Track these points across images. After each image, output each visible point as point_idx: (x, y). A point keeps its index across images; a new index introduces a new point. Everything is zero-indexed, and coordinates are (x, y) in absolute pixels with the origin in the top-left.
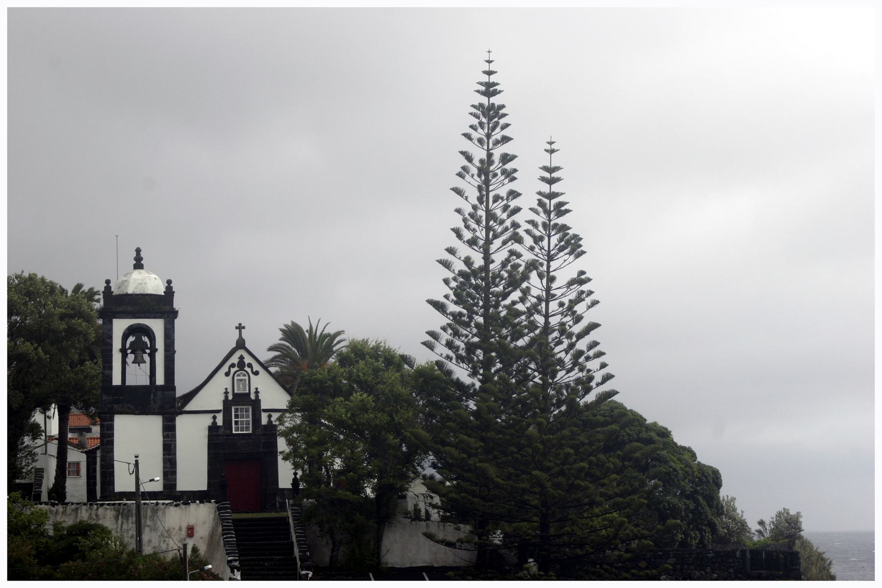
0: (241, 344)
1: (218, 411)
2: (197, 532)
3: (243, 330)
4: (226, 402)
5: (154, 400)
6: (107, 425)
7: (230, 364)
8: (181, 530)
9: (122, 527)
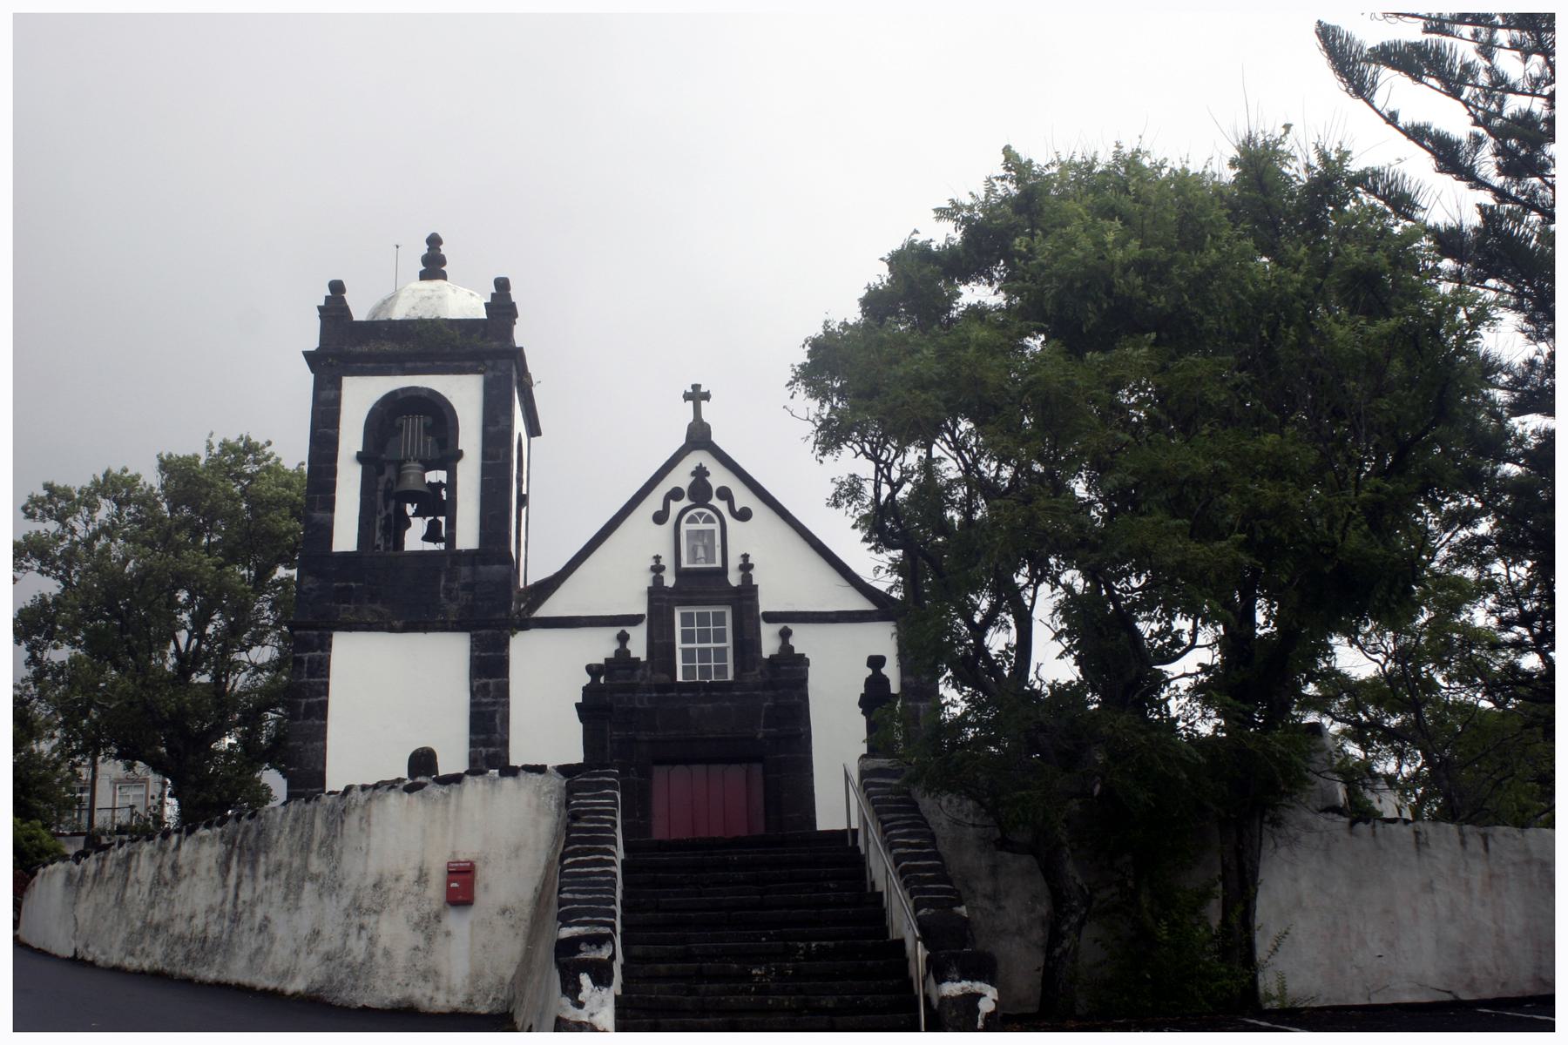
0: (699, 437)
1: (634, 620)
2: (486, 887)
3: (704, 403)
4: (656, 593)
5: (449, 591)
7: (669, 489)
8: (427, 881)
9: (237, 896)
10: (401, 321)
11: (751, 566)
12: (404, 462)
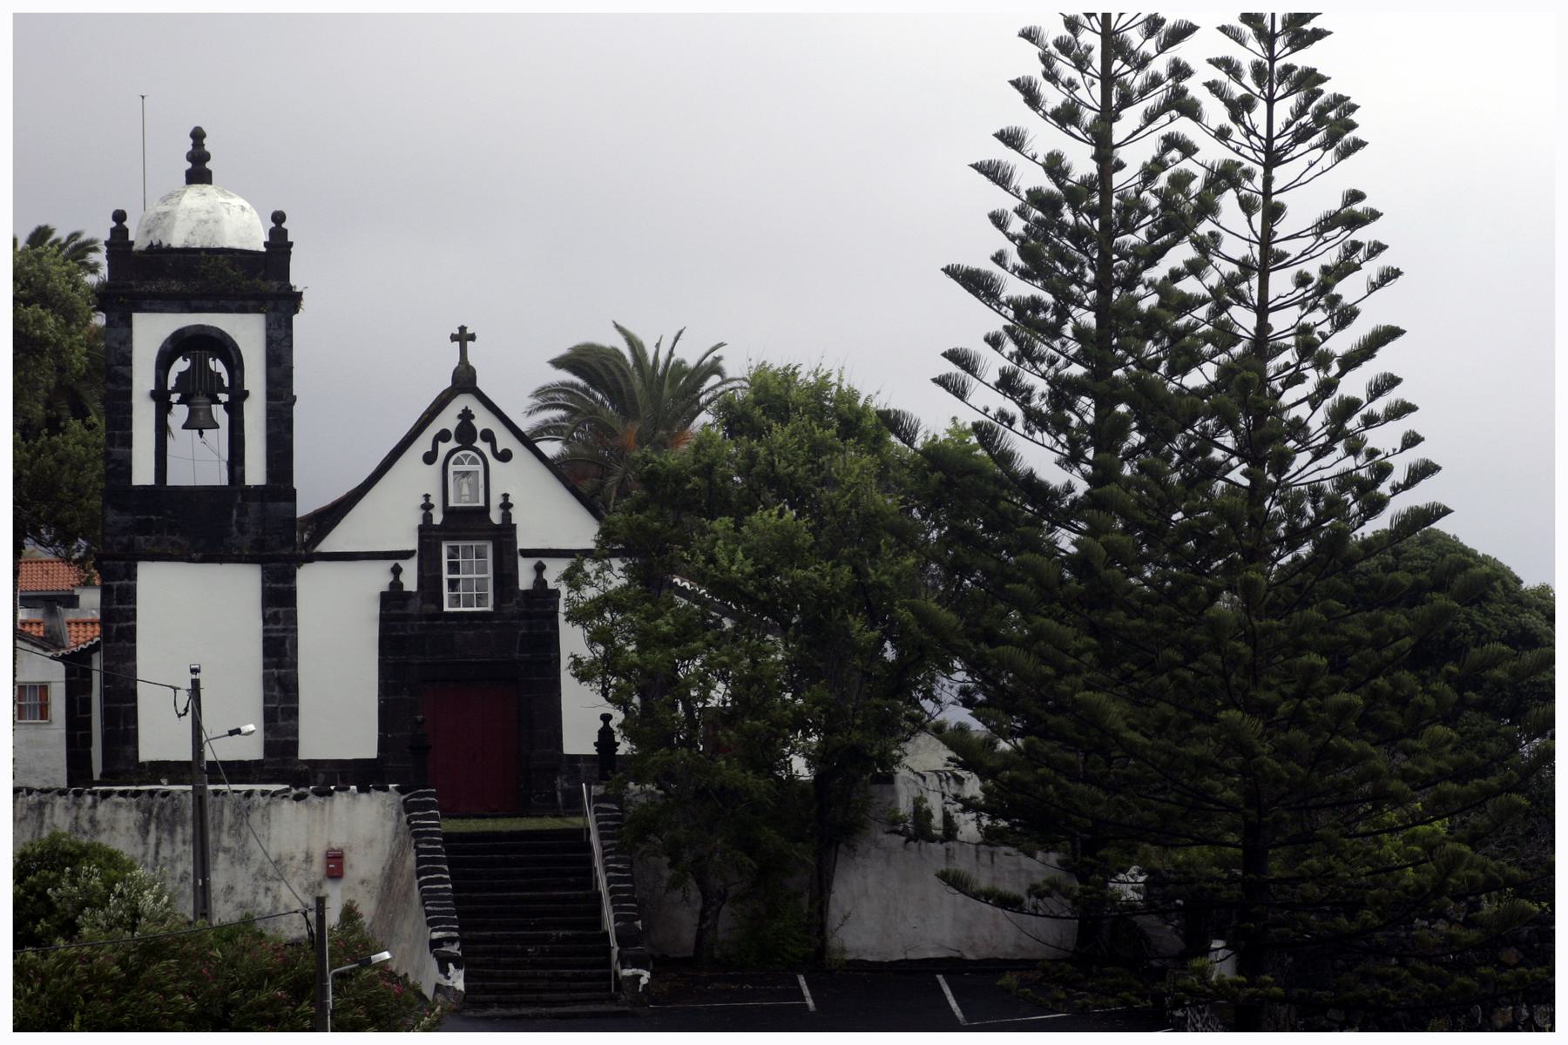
0: (464, 380)
1: (406, 555)
2: (351, 867)
3: (469, 344)
4: (426, 530)
6: (119, 588)
7: (438, 431)
8: (311, 861)
9: (157, 853)
10: (186, 251)
11: (511, 505)
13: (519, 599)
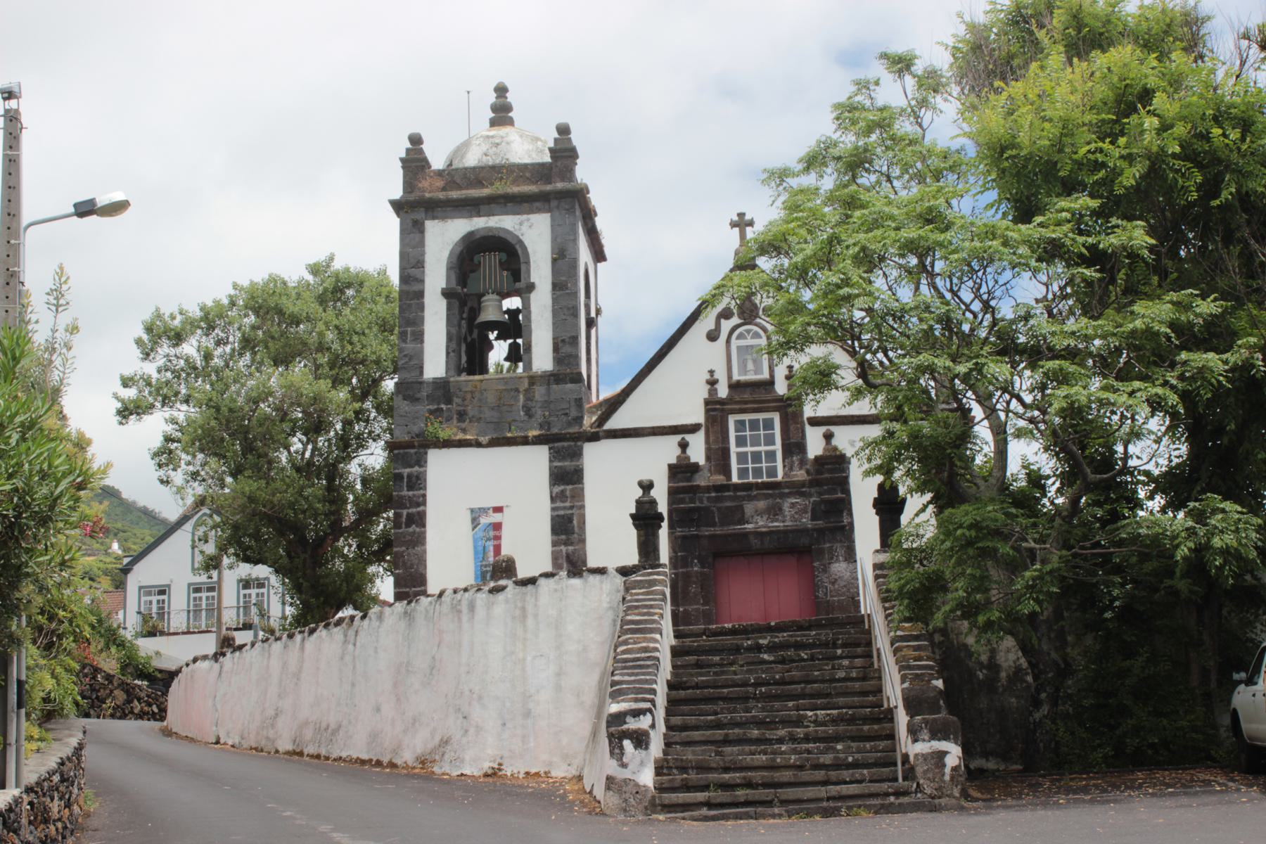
1: (693, 429)
3: (748, 229)
6: (409, 476)
10: (474, 168)
12: (483, 295)
13: (808, 467)
